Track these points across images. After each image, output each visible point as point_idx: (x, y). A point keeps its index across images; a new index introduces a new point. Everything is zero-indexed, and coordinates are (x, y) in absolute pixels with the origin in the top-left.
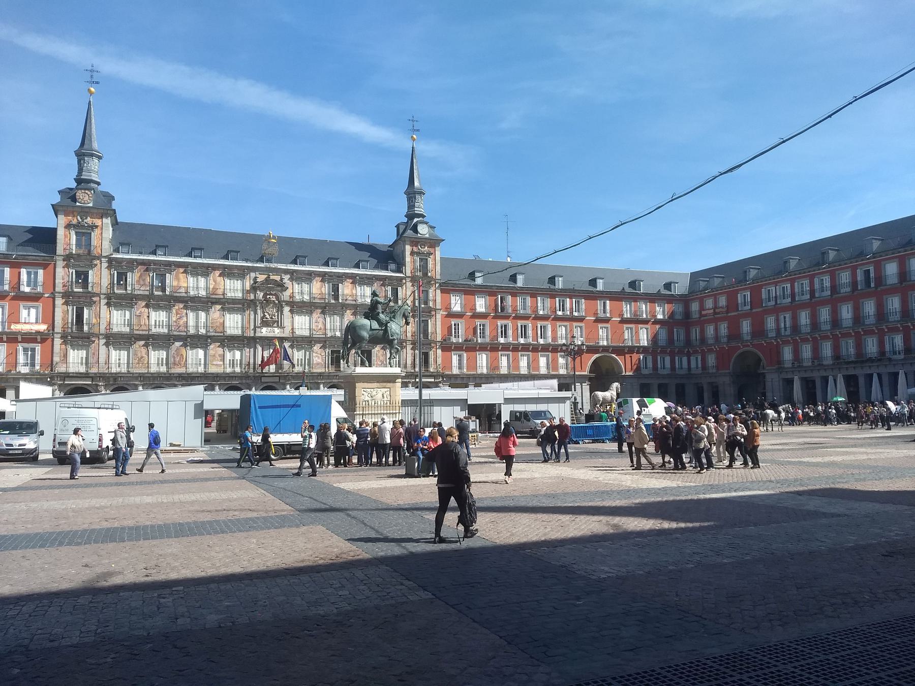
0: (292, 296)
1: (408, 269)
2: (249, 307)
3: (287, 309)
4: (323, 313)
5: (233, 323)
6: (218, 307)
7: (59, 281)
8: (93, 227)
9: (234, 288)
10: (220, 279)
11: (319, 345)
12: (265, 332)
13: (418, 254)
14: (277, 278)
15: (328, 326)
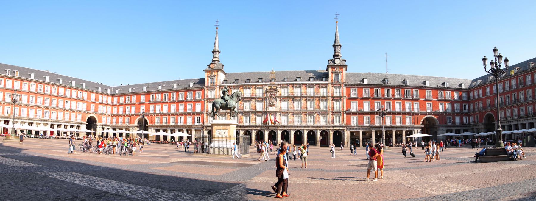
0: (280, 94)
1: (330, 80)
2: (264, 100)
3: (278, 100)
4: (293, 100)
5: (259, 106)
6: (254, 100)
7: (206, 95)
8: (215, 76)
9: (260, 93)
10: (254, 90)
11: (291, 114)
12: (270, 109)
13: (335, 72)
14: (275, 88)
15: (295, 106)
